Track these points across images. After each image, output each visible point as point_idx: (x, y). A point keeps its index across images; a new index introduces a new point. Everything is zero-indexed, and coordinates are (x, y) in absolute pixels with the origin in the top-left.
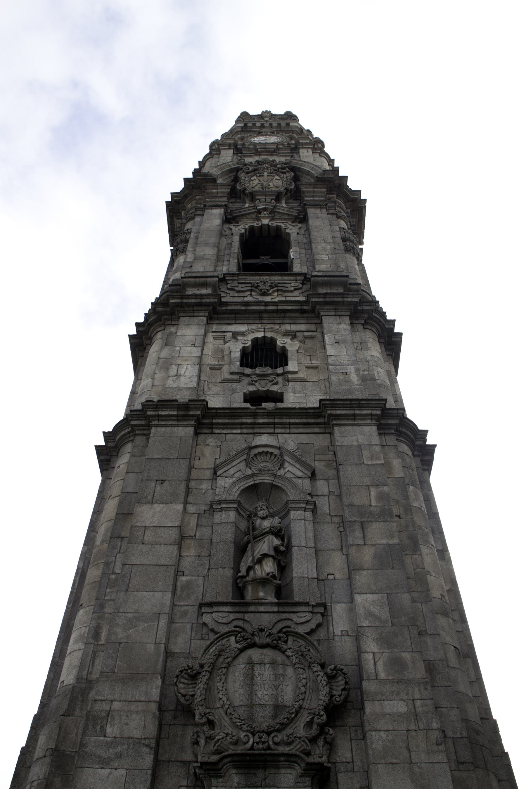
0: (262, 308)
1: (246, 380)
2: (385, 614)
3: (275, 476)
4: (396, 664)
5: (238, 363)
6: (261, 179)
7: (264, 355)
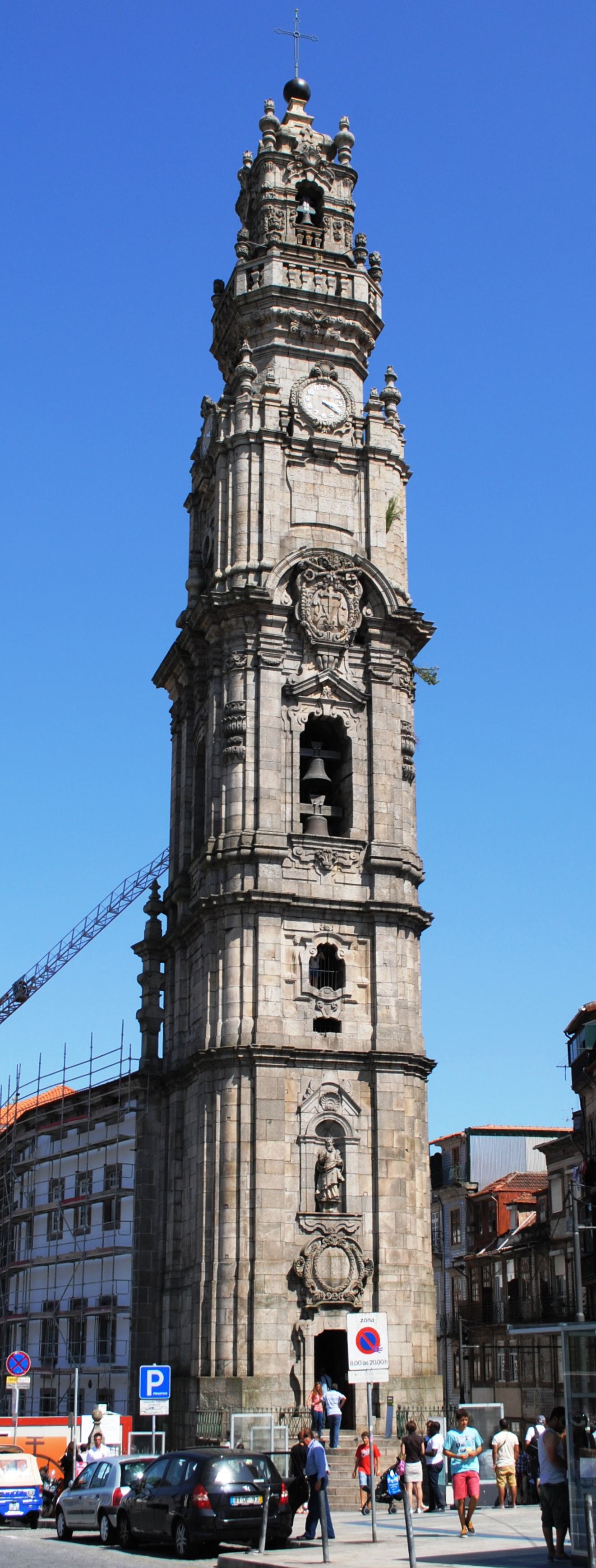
0: (328, 906)
1: (313, 1001)
2: (392, 1225)
3: (336, 1115)
4: (395, 1255)
5: (308, 981)
6: (325, 601)
7: (328, 970)
